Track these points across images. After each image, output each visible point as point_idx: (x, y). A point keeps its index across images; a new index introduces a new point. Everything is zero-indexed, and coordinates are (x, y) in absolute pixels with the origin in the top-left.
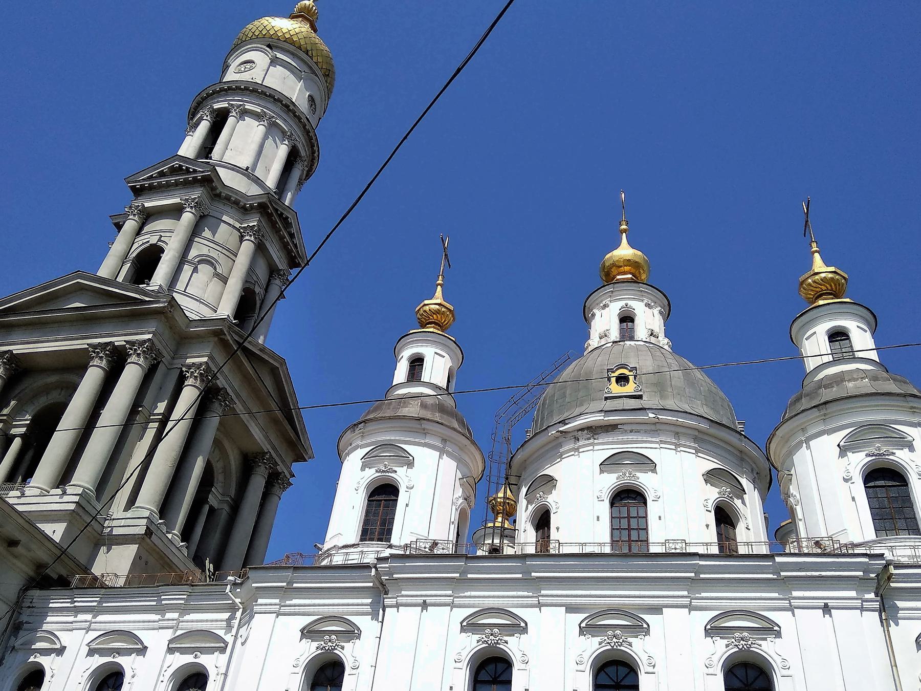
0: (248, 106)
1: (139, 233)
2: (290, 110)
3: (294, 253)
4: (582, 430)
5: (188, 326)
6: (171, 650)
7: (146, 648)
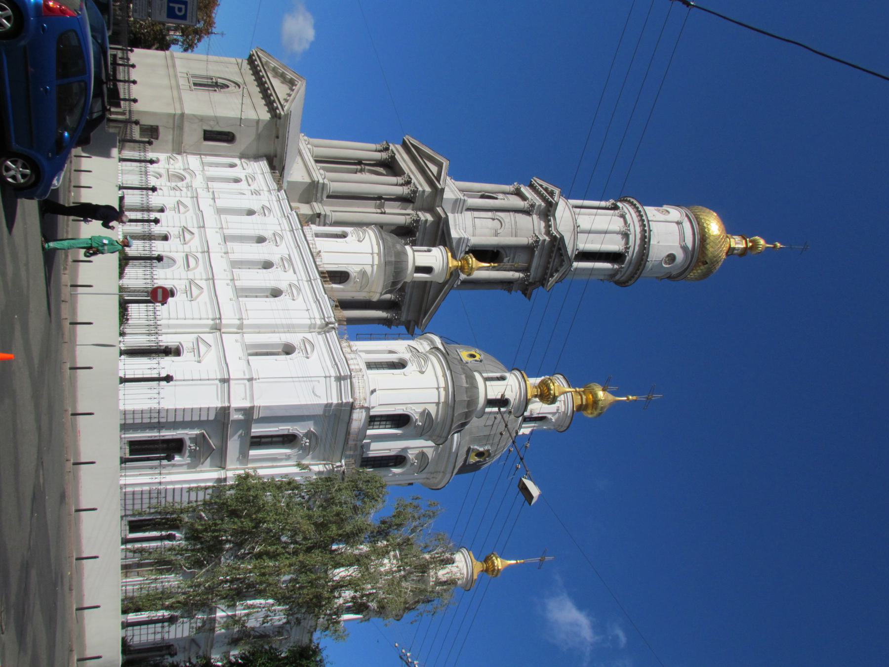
0: (628, 217)
1: (504, 193)
5: (438, 207)
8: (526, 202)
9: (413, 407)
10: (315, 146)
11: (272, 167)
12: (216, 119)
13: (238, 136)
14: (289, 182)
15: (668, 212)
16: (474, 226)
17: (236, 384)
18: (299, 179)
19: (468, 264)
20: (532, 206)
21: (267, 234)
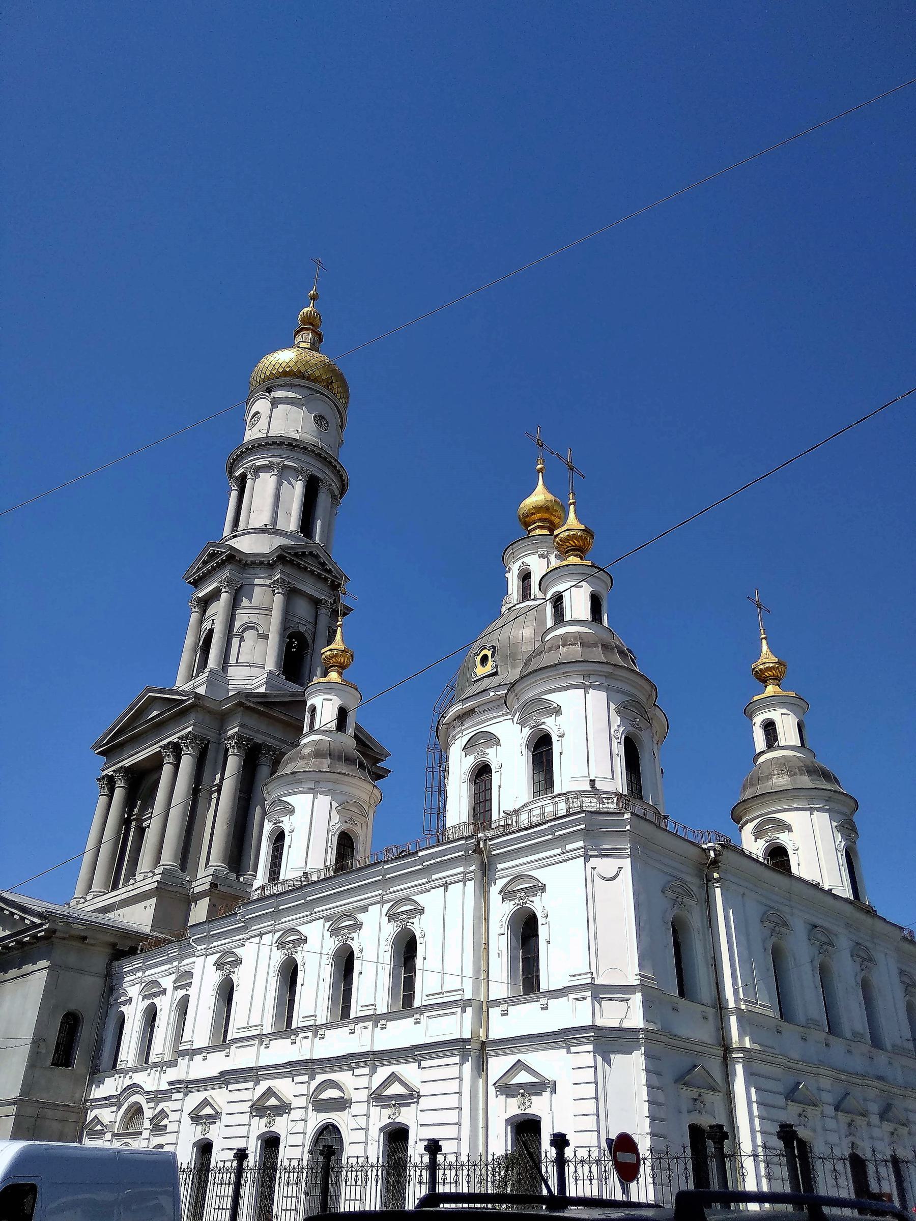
0: (259, 463)
1: (201, 622)
2: (294, 446)
3: (330, 578)
4: (455, 720)
6: (176, 988)
7: (166, 989)
8: (223, 590)
9: (614, 727)
10: (90, 887)
11: (132, 952)
12: (37, 1042)
13: (72, 1007)
14: (153, 928)
15: (257, 413)
16: (248, 665)
17: (602, 1016)
18: (150, 912)
19: (337, 655)
20: (229, 582)
21: (278, 957)
